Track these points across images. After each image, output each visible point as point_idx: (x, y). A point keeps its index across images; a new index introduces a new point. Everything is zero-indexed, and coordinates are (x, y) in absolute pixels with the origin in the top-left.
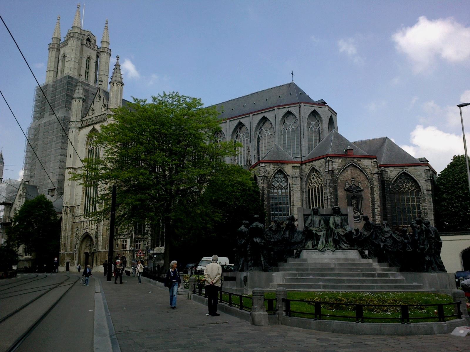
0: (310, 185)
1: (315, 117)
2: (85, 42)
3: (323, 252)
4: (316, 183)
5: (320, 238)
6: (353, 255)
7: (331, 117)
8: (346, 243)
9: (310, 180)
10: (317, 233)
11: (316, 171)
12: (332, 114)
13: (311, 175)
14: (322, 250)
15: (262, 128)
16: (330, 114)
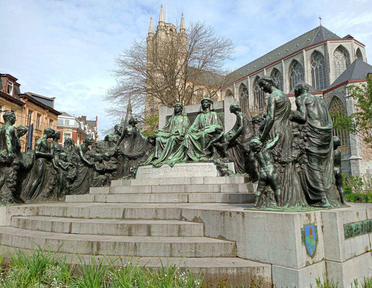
0: (333, 112)
1: (342, 51)
2: (168, 32)
4: (338, 110)
7: (358, 49)
8: (200, 153)
9: (333, 108)
11: (338, 99)
12: (360, 47)
13: (334, 103)
15: (293, 70)
16: (356, 47)
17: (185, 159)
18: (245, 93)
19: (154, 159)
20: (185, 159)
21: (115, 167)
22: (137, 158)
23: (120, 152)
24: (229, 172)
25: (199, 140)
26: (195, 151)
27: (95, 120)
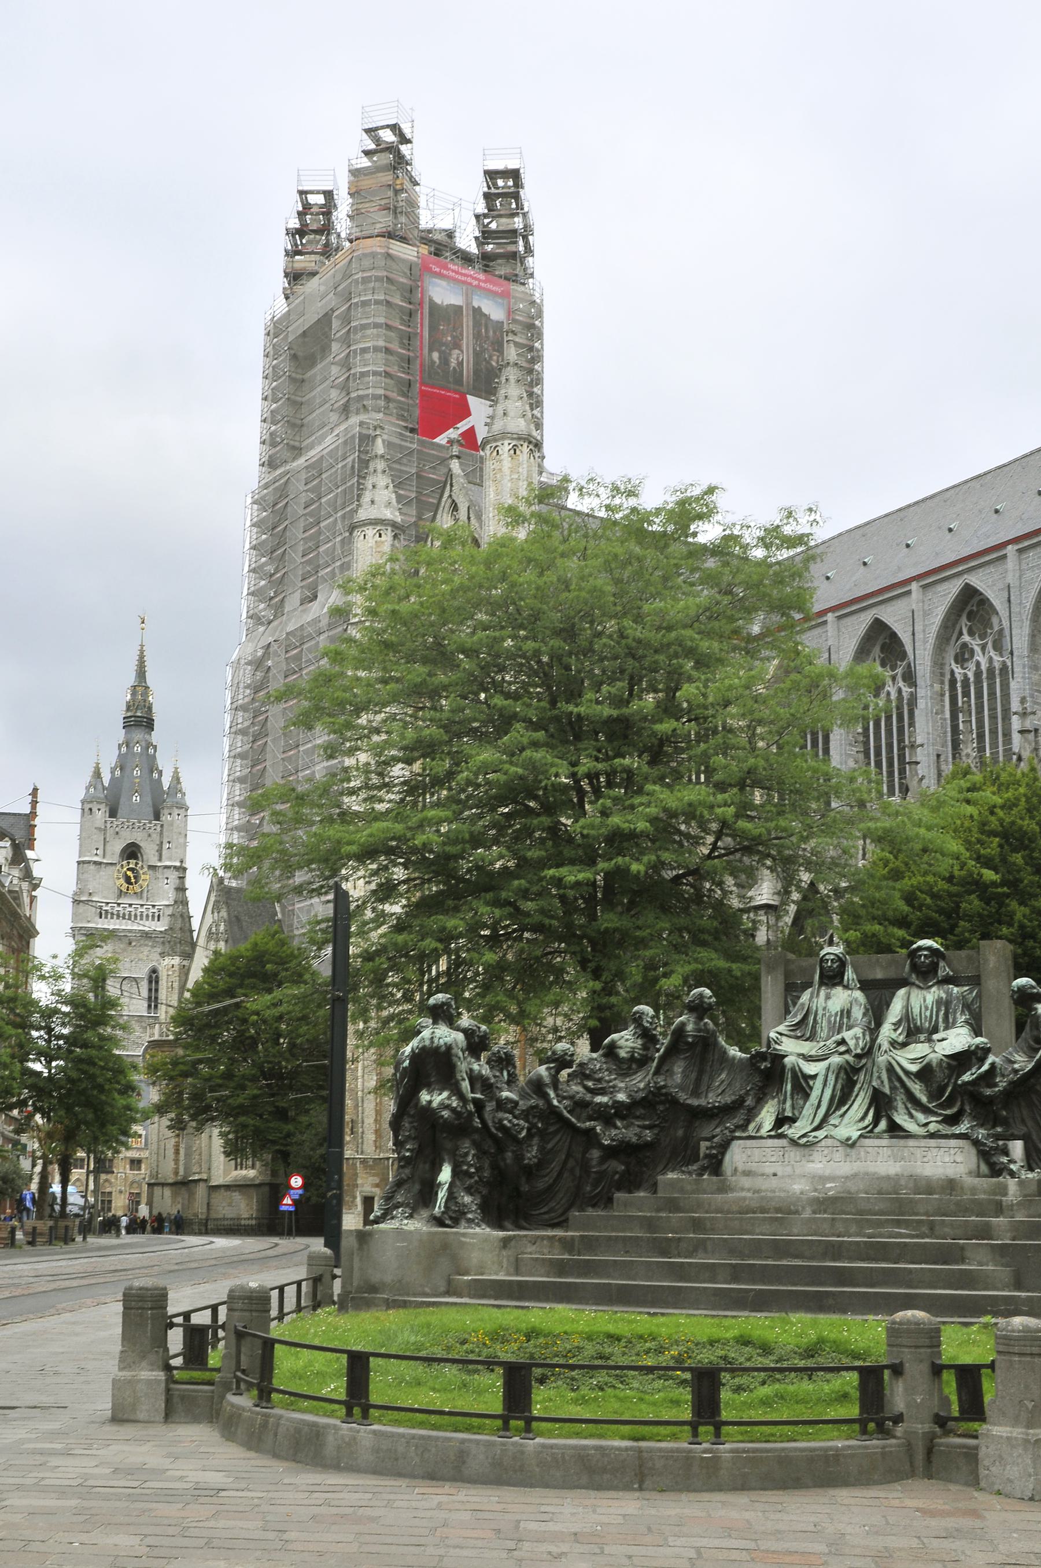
3: (807, 1151)
5: (811, 1088)
6: (944, 1159)
8: (926, 1110)
14: (803, 1141)
17: (883, 1125)
18: (894, 678)
19: (781, 1121)
20: (883, 1125)
21: (648, 1135)
22: (717, 1115)
23: (666, 1094)
24: (1012, 1166)
25: (925, 1074)
27: (27, 810)
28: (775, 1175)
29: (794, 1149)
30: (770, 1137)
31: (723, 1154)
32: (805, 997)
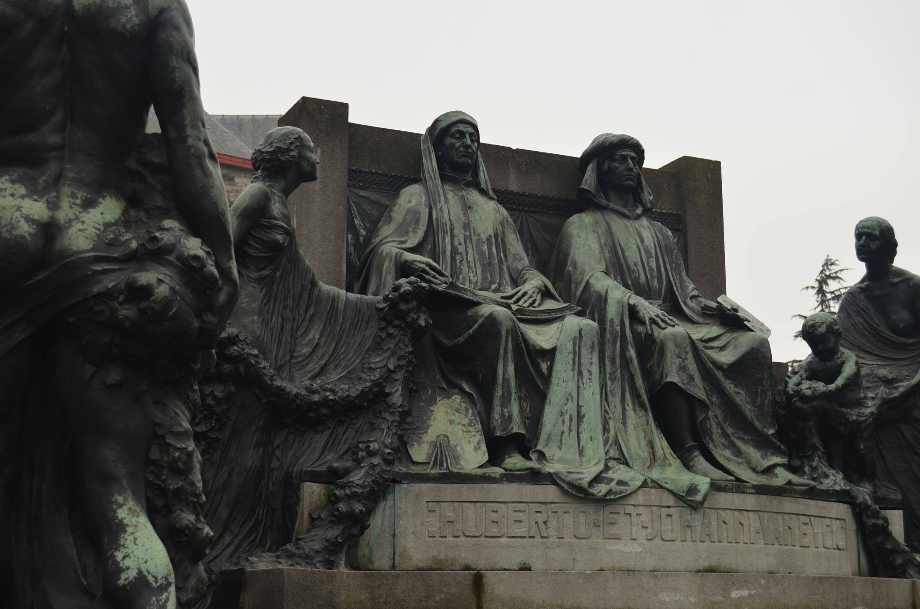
3: (604, 514)
5: (547, 379)
10: (524, 327)
14: (601, 489)
26: (730, 430)
28: (526, 568)
29: (572, 507)
30: (511, 477)
31: (370, 511)
32: (411, 197)
